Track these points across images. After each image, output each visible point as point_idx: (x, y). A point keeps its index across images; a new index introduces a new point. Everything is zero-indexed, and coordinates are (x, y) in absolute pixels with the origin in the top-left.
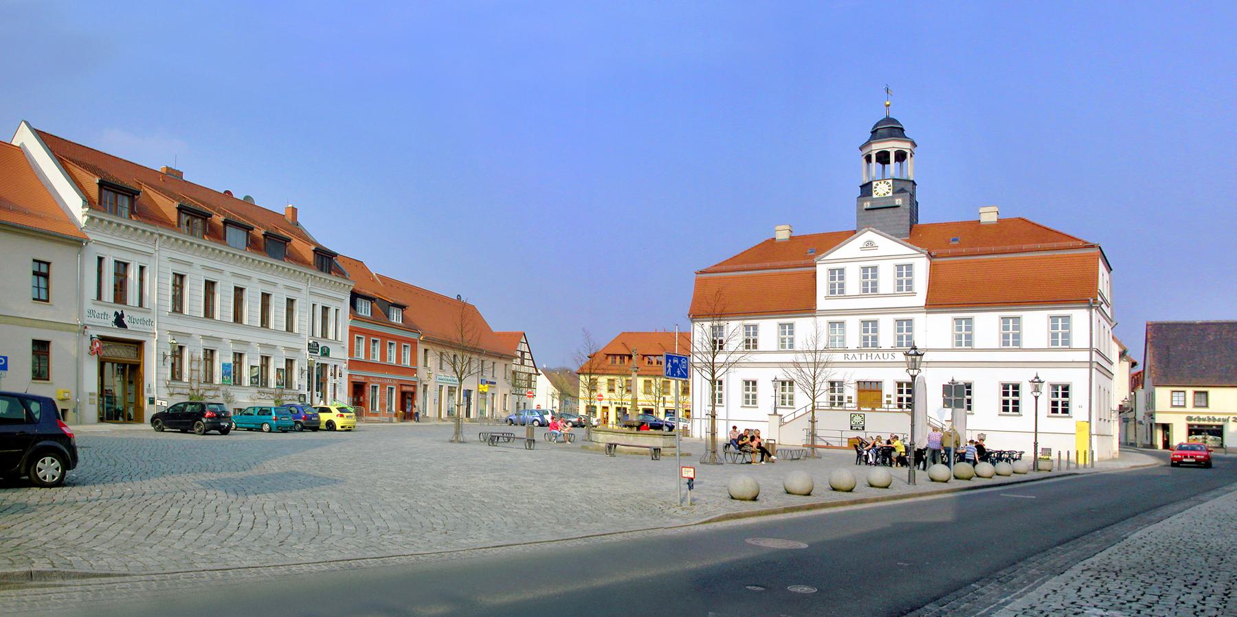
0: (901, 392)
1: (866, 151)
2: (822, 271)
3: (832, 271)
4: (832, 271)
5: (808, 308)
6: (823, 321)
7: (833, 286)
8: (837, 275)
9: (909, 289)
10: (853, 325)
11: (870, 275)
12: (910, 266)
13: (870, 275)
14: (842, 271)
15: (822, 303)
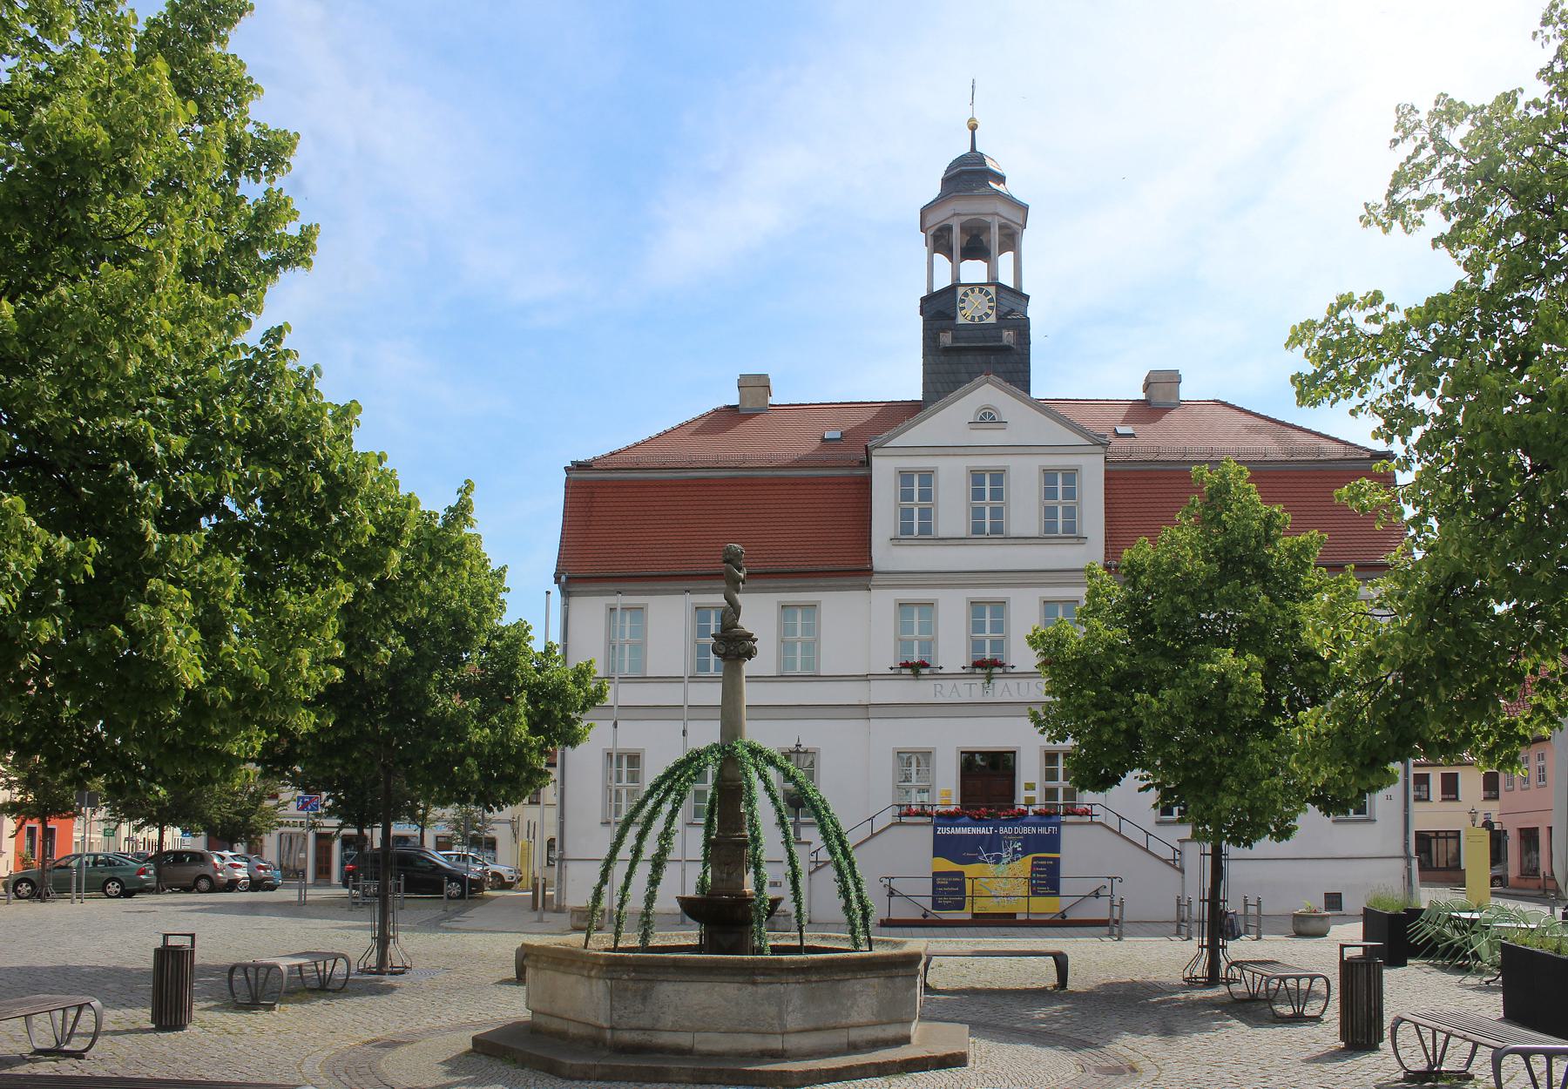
0: (1051, 775)
1: (936, 218)
2: (884, 472)
3: (905, 476)
4: (905, 476)
5: (855, 569)
6: (881, 603)
7: (906, 514)
8: (918, 485)
9: (1070, 528)
10: (952, 608)
11: (988, 485)
12: (1071, 475)
13: (988, 485)
14: (927, 476)
15: (884, 554)
